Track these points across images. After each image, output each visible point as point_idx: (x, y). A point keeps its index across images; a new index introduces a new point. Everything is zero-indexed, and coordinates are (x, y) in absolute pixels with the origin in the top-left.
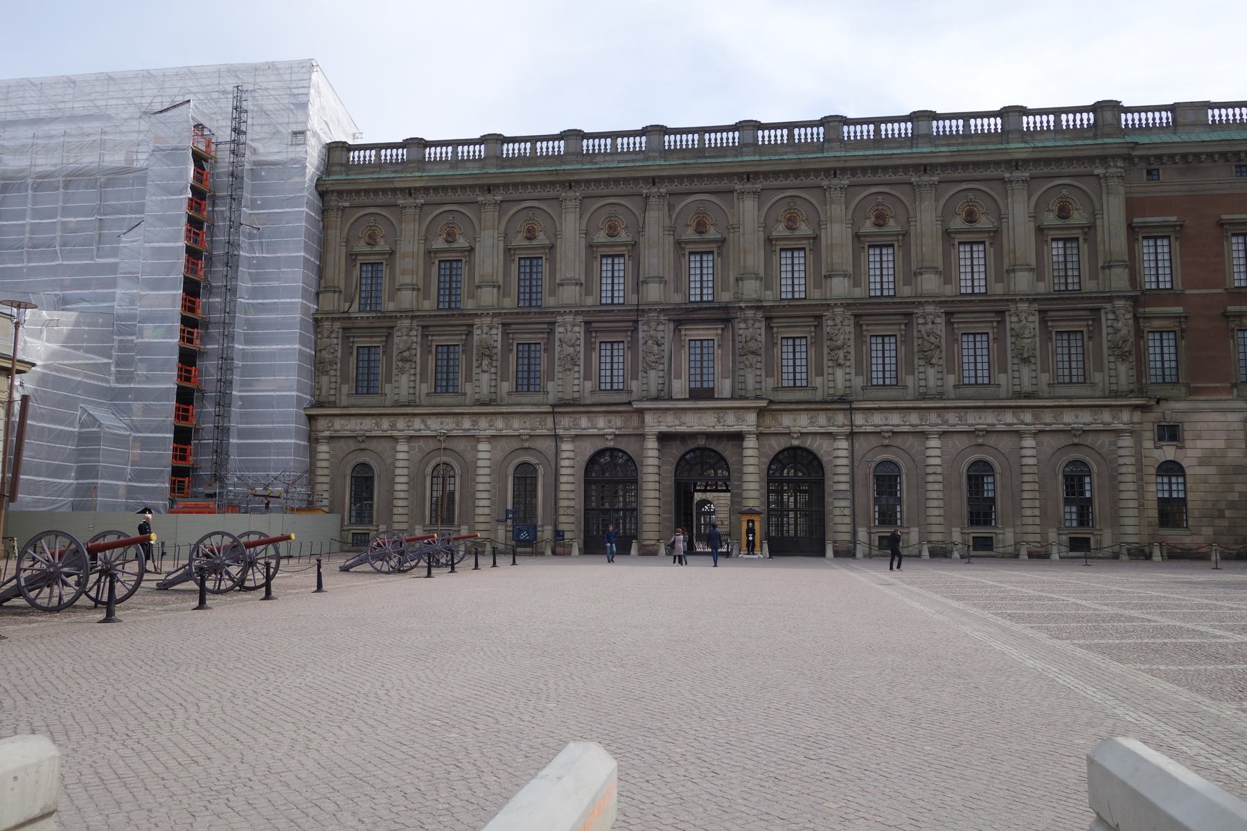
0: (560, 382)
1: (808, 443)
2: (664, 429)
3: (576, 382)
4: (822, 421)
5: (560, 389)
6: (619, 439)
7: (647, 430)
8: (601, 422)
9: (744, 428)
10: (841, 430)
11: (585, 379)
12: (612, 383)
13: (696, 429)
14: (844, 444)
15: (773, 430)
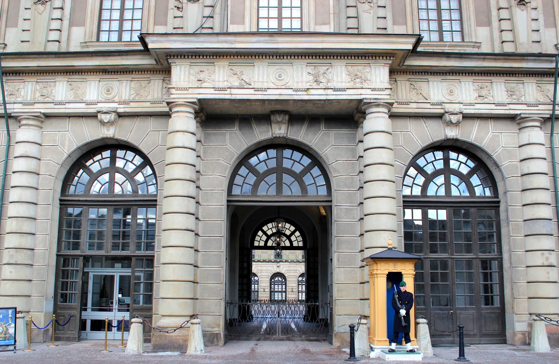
0: (27, 25)
1: (473, 134)
2: (208, 94)
3: (55, 25)
4: (498, 94)
5: (26, 36)
6: (127, 122)
7: (176, 96)
8: (93, 93)
9: (366, 95)
10: (533, 110)
11: (71, 25)
12: (121, 31)
13: (273, 94)
14: (537, 135)
15: (412, 108)
